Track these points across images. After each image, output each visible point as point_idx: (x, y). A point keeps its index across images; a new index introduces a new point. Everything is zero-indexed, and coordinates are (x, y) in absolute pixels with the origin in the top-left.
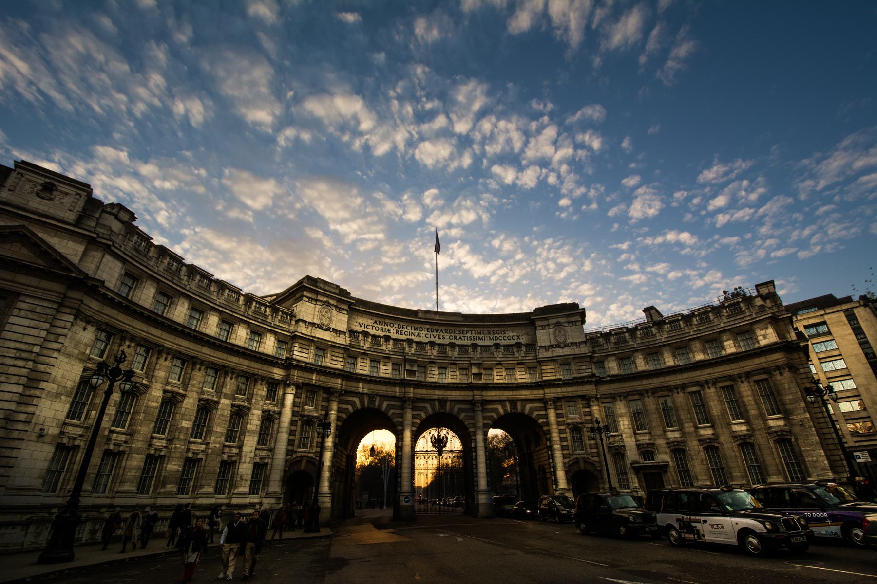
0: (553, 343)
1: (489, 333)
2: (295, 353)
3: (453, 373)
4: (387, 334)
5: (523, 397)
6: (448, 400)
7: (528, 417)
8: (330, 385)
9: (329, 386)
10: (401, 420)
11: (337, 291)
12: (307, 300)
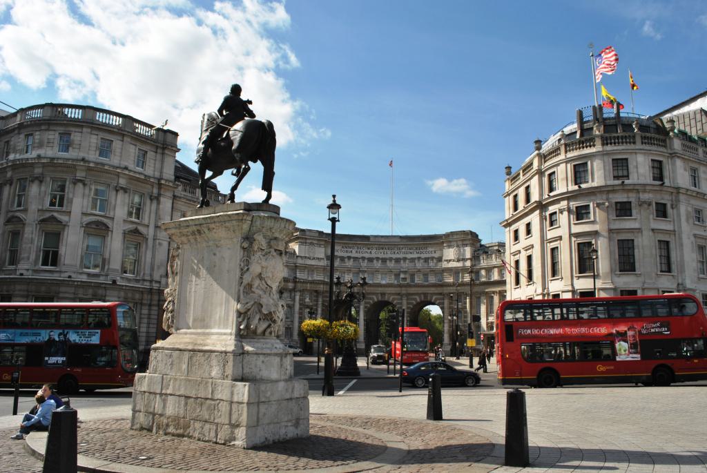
1: (416, 249)
2: (298, 275)
4: (349, 254)
5: (431, 292)
8: (317, 289)
11: (317, 234)
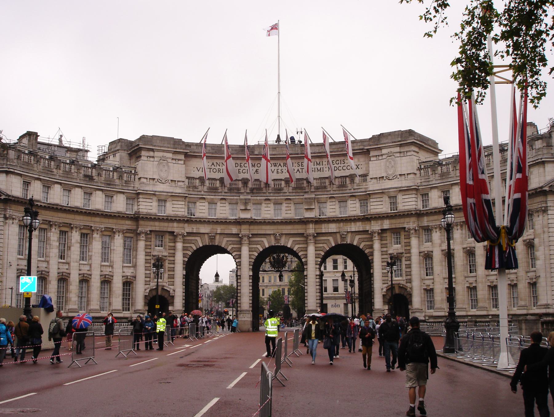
0: (384, 175)
3: (288, 208)
5: (353, 230)
6: (282, 234)
7: (357, 248)
9: (172, 230)
10: (238, 253)
12: (145, 158)
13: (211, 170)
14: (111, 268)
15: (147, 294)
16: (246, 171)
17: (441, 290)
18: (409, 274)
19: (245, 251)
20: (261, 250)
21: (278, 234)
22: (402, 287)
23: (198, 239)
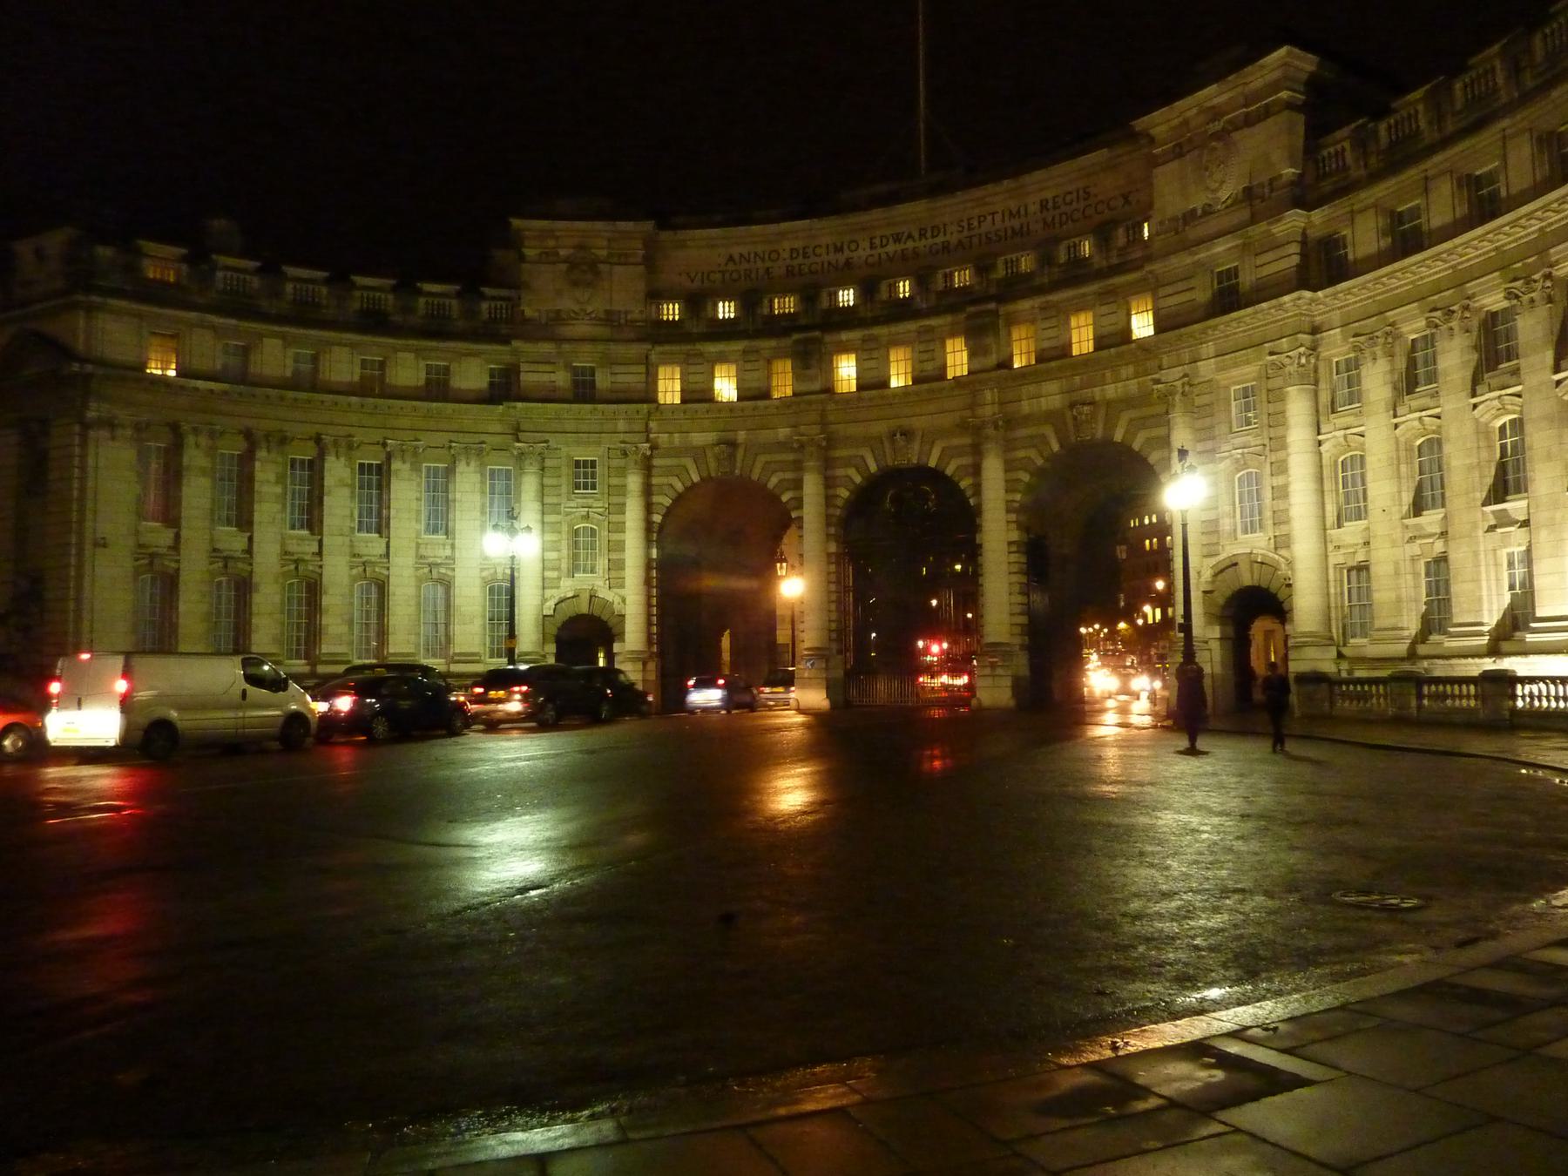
3: (925, 356)
13: (727, 275)
14: (448, 547)
15: (551, 612)
16: (819, 268)
17: (1396, 563)
18: (1281, 519)
19: (812, 486)
20: (858, 479)
21: (898, 436)
22: (1262, 563)
23: (689, 463)
